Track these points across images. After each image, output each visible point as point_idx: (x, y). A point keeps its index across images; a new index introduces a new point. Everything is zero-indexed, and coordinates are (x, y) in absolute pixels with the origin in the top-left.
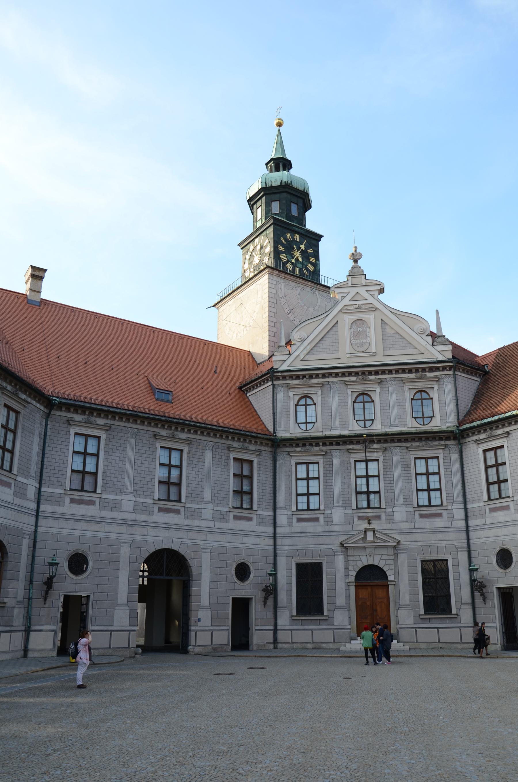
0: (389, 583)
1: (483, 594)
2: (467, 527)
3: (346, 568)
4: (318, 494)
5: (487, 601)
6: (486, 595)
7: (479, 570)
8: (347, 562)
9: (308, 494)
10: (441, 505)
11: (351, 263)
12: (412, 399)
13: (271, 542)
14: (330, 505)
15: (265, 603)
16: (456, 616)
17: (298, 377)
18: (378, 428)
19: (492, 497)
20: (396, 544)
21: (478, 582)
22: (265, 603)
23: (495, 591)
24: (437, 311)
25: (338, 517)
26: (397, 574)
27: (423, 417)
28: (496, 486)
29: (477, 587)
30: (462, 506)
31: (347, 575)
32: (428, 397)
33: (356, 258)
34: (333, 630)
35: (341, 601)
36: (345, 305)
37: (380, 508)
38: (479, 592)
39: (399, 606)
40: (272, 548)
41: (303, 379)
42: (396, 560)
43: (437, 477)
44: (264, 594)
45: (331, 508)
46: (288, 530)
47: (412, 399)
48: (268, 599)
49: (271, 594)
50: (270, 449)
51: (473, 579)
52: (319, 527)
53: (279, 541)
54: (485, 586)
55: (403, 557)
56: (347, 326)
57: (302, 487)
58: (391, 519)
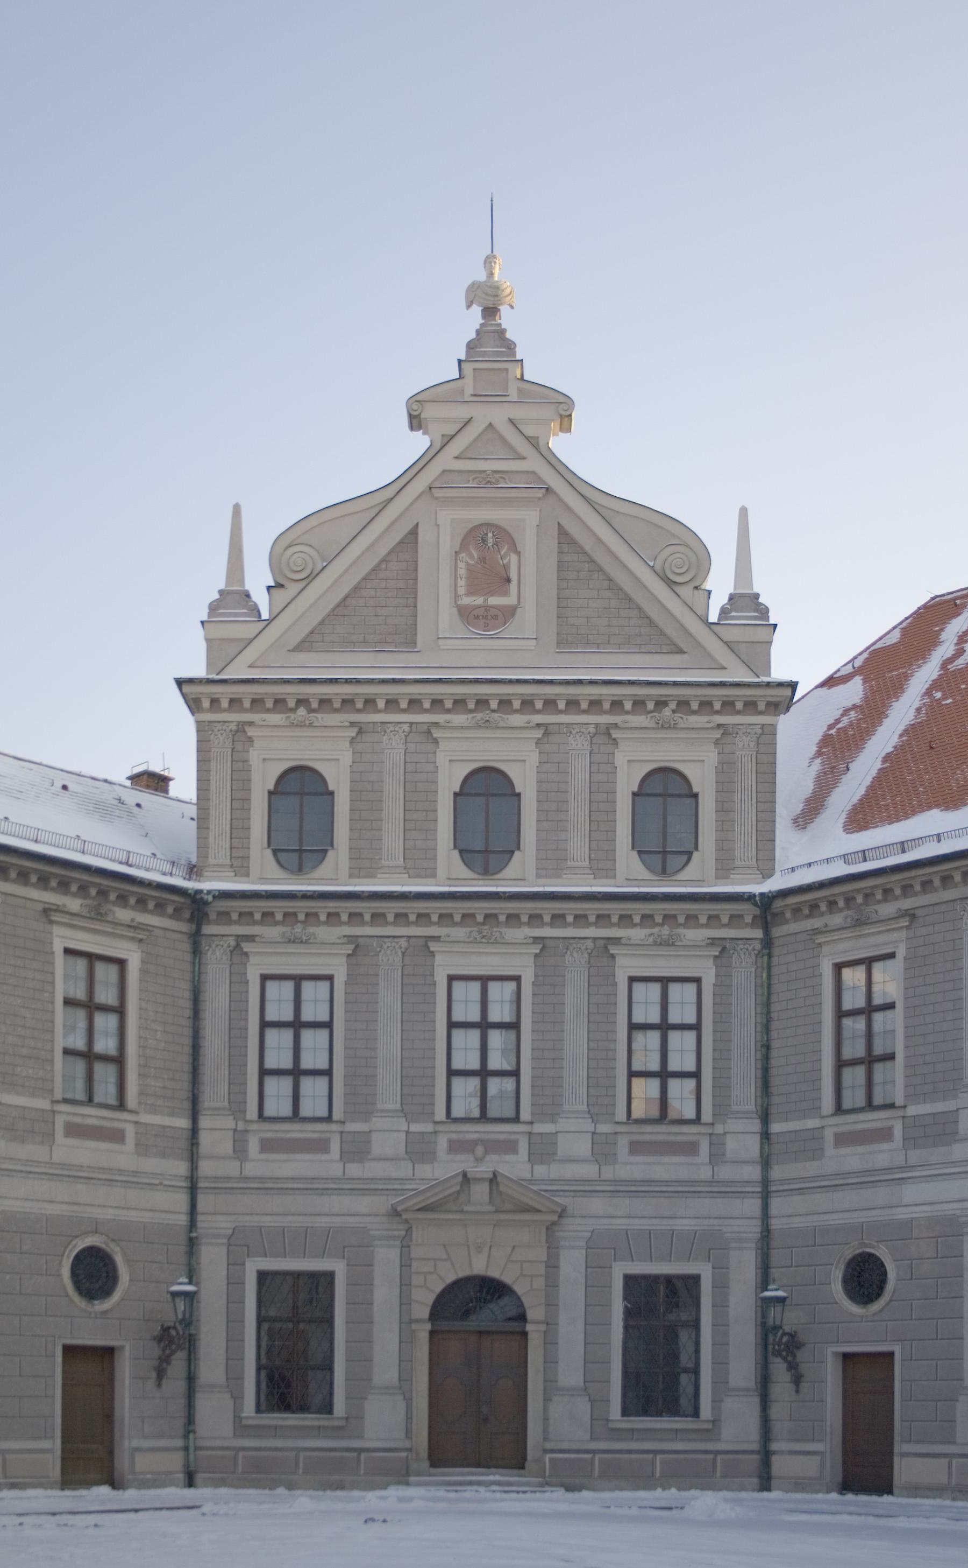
0: (529, 1327)
1: (793, 1367)
2: (765, 1182)
3: (405, 1285)
4: (328, 1073)
5: (804, 1386)
6: (803, 1368)
7: (788, 1302)
8: (405, 1264)
9: (296, 1073)
10: (697, 1120)
11: (475, 316)
12: (634, 794)
13: (181, 1200)
14: (363, 1105)
15: (161, 1374)
16: (710, 1426)
17: (279, 703)
18: (521, 874)
19: (847, 1104)
20: (555, 1218)
21: (784, 1334)
22: (161, 1374)
23: (830, 1359)
24: (744, 512)
25: (388, 1135)
26: (551, 1304)
27: (664, 853)
28: (860, 1071)
29: (779, 1345)
30: (756, 1126)
31: (405, 1302)
32: (686, 791)
33: (488, 300)
34: (360, 1451)
35: (385, 1369)
36: (444, 471)
37: (516, 1119)
38: (785, 1359)
39: (551, 1388)
40: (183, 1219)
41: (293, 710)
42: (552, 1266)
43: (691, 1036)
44: (155, 1350)
45: (366, 1116)
46: (232, 1169)
47: (635, 795)
48: (169, 1363)
49: (180, 1348)
50: (183, 927)
51: (770, 1322)
52: (329, 1164)
53: (203, 1202)
54: (800, 1346)
55: (572, 1264)
56: (448, 544)
57: (279, 1050)
58: (543, 1150)
